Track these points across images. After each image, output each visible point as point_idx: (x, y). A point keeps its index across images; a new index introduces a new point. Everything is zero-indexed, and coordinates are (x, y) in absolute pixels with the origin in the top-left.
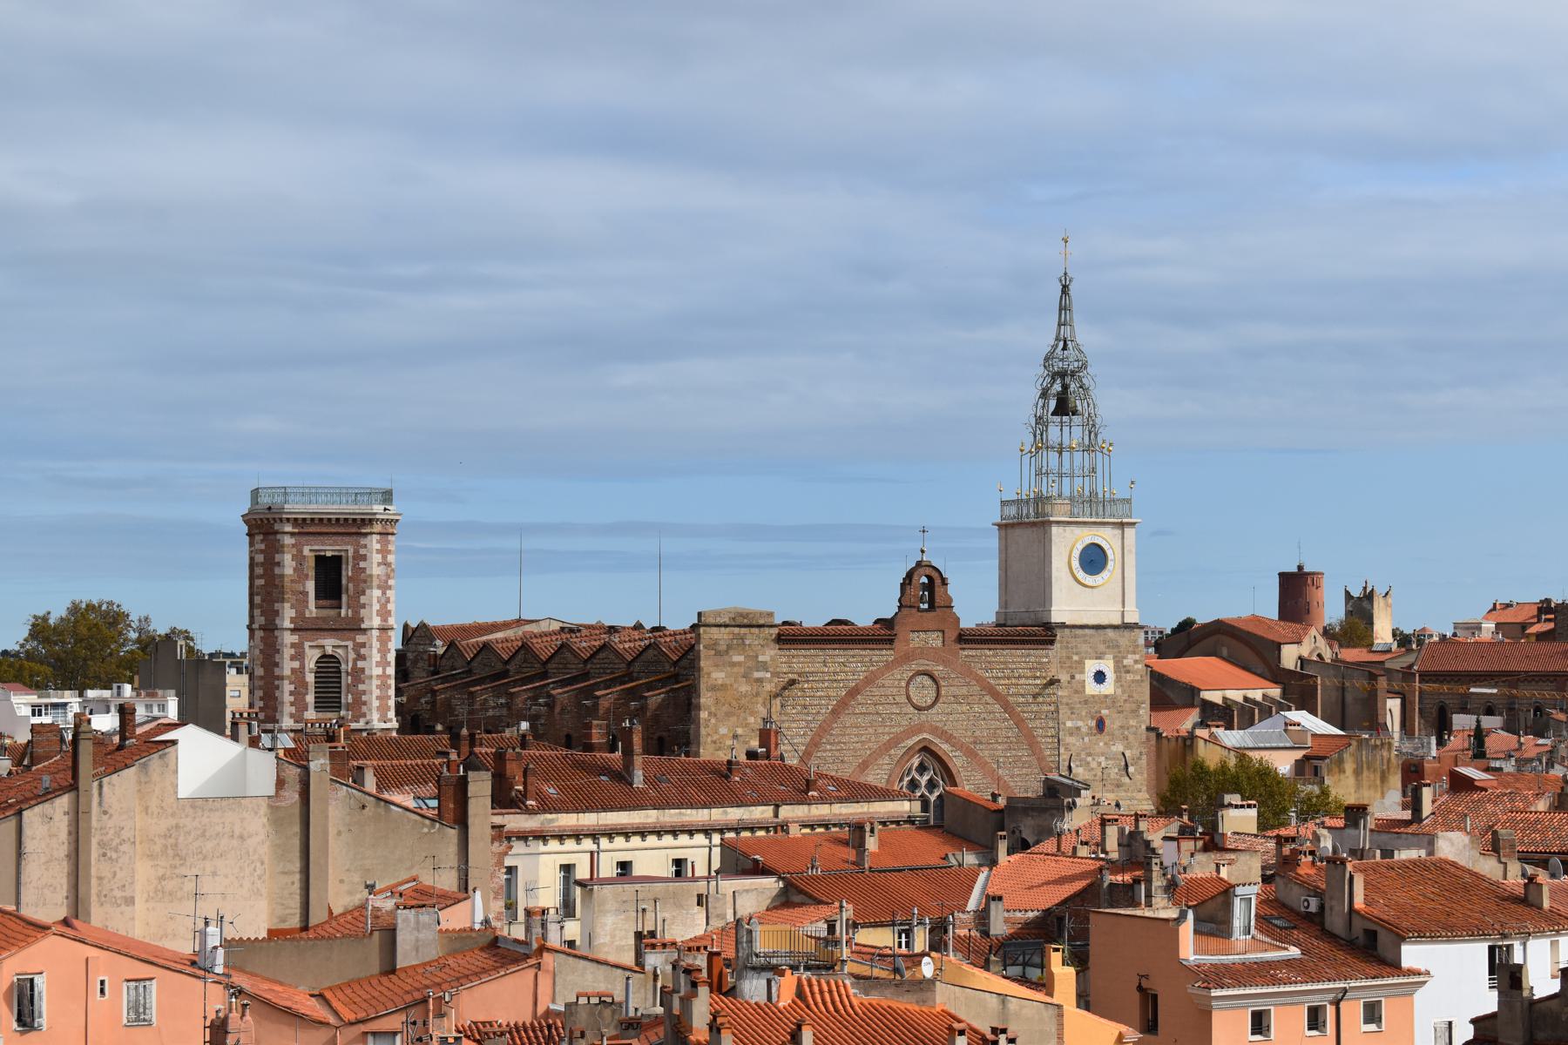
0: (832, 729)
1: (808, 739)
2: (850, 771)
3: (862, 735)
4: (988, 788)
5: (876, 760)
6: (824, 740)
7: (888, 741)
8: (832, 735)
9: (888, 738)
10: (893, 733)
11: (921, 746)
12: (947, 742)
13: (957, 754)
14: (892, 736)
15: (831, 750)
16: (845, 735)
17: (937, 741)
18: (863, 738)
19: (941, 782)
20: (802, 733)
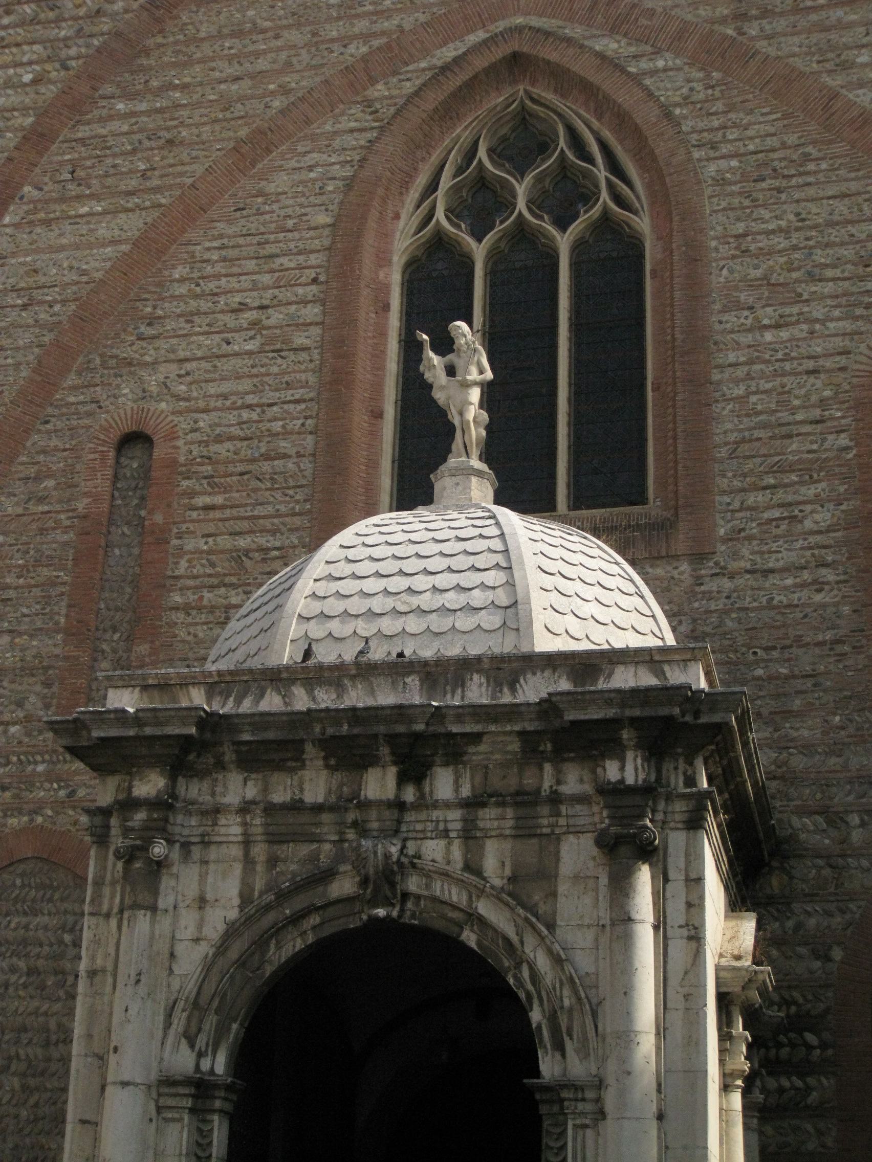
0: (147, 52)
1: (49, 91)
2: (198, 169)
3: (257, 54)
4: (807, 157)
5: (308, 122)
6: (109, 89)
7: (364, 59)
8: (143, 69)
9: (364, 49)
10: (383, 33)
11: (499, 52)
12: (613, 30)
13: (660, 64)
14: (376, 43)
15: (133, 114)
16: (189, 63)
17: (575, 31)
18: (262, 64)
19: (602, 173)
20: (27, 78)
